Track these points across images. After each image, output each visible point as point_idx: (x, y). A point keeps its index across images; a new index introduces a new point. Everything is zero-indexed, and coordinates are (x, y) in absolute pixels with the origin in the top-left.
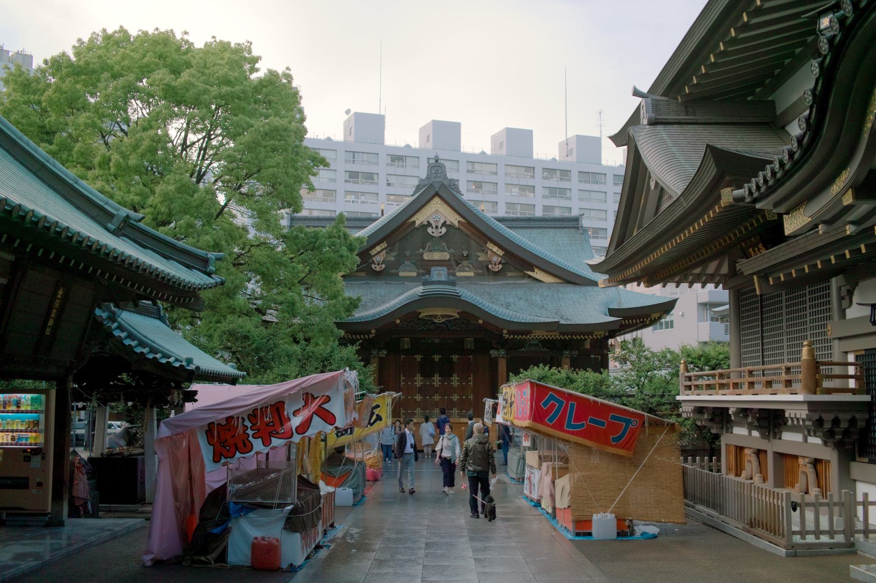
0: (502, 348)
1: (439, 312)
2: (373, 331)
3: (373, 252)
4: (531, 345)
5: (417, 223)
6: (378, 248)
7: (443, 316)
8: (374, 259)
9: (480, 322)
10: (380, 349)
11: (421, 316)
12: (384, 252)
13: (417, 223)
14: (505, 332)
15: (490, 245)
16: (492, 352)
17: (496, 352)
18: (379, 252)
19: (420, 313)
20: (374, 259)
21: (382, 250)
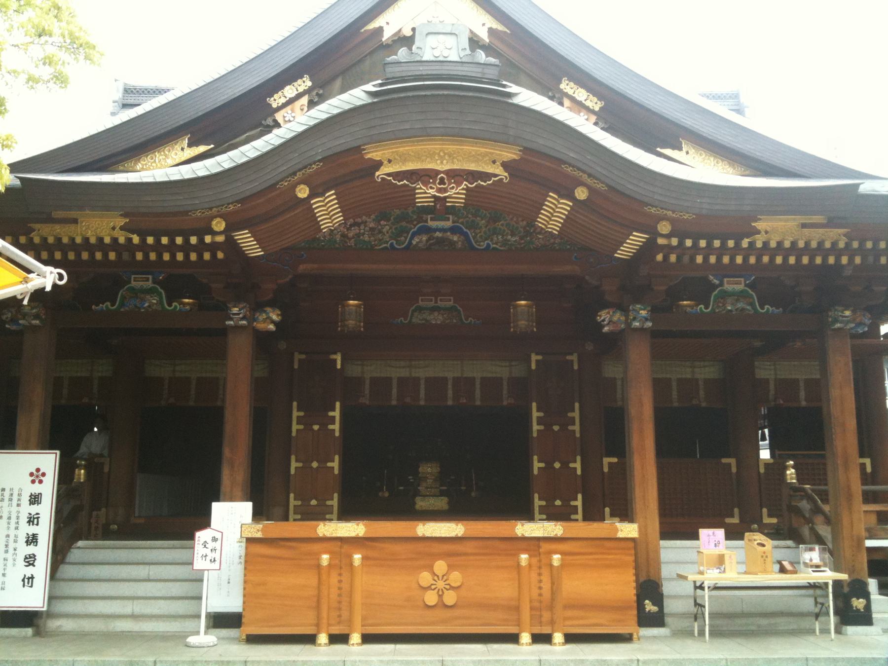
0: (637, 301)
1: (439, 156)
2: (219, 225)
3: (277, 100)
4: (725, 295)
5: (387, 35)
6: (289, 91)
7: (456, 176)
8: (279, 117)
9: (581, 194)
10: (258, 307)
11: (380, 173)
12: (305, 100)
13: (387, 35)
14: (664, 228)
15: (566, 86)
16: (604, 316)
17: (618, 316)
18: (291, 101)
19: (378, 165)
20: (279, 117)
21: (299, 96)
